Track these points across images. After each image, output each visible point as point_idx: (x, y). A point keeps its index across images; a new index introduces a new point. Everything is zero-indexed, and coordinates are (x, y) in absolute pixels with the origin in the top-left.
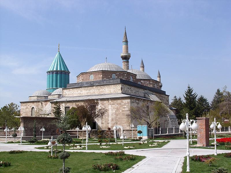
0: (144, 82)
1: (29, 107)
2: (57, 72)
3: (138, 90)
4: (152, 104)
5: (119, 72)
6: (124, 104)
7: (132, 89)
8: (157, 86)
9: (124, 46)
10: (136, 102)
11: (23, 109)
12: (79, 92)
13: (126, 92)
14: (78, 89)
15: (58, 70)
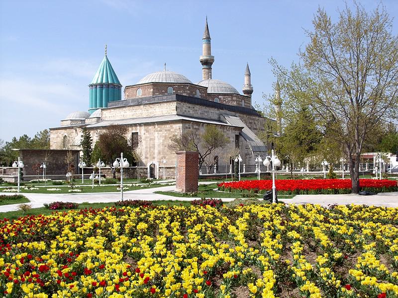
0: (224, 98)
1: (60, 135)
2: (102, 85)
3: (207, 109)
4: (225, 130)
5: (178, 84)
6: (173, 130)
7: (195, 108)
8: (246, 104)
9: (204, 46)
10: (193, 127)
11: (53, 138)
12: (123, 113)
13: (185, 113)
14: (121, 110)
15: (104, 82)
